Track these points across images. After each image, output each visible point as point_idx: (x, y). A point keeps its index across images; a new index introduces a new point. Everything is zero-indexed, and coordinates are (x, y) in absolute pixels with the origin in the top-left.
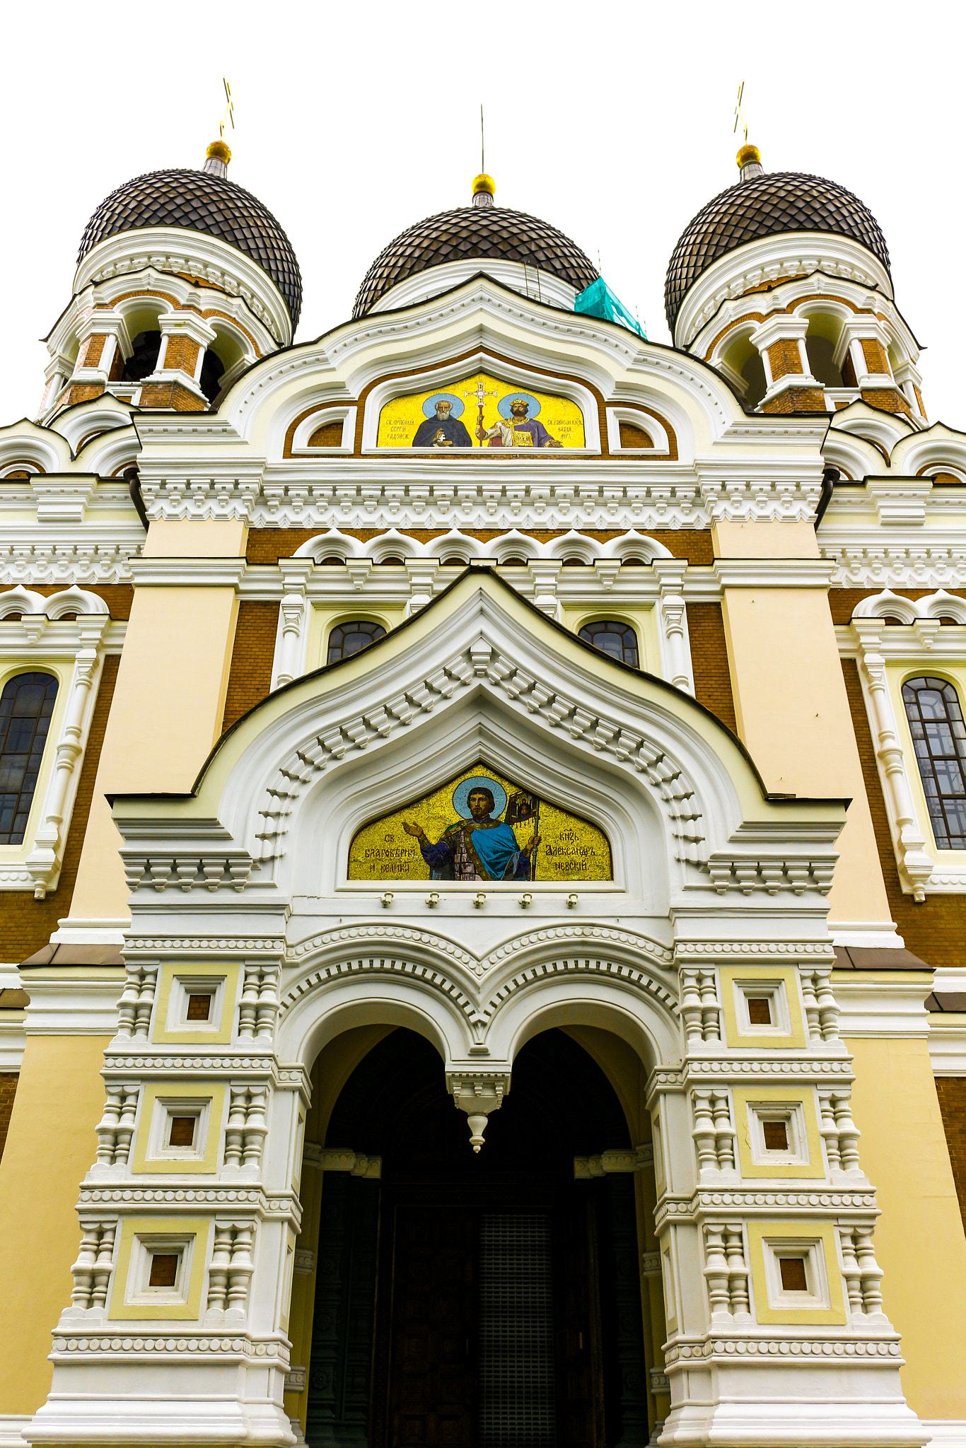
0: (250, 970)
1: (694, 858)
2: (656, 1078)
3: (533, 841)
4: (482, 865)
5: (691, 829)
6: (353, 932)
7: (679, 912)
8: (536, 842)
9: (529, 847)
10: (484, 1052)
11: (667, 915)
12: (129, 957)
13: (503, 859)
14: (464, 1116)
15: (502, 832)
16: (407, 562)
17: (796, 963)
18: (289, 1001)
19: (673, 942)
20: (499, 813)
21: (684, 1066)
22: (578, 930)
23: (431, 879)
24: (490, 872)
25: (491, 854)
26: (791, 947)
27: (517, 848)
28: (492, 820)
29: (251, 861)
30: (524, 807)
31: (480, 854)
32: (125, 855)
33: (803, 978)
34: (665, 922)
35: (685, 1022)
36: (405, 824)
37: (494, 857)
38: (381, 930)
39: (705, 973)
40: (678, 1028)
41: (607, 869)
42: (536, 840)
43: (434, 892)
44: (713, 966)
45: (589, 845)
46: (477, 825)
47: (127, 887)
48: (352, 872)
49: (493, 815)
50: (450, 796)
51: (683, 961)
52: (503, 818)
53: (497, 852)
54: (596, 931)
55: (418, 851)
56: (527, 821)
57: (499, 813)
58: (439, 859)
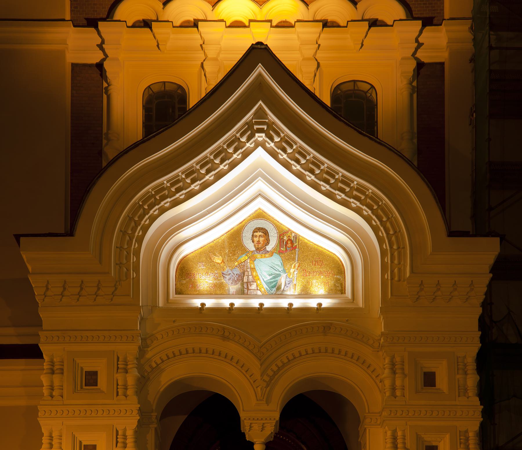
24: (267, 289)
28: (268, 252)
30: (289, 242)
46: (258, 256)
49: (269, 248)
53: (272, 275)
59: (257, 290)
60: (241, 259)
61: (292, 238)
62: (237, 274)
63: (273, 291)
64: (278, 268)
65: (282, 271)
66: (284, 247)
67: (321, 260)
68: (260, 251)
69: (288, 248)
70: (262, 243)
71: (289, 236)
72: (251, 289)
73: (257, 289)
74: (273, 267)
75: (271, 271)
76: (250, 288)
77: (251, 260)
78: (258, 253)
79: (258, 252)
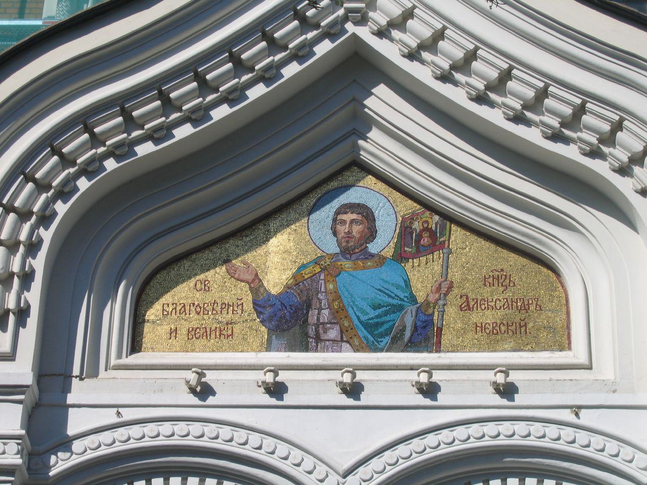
3: (439, 289)
9: (432, 298)
13: (388, 318)
15: (389, 274)
23: (268, 349)
25: (369, 310)
27: (413, 299)
28: (372, 255)
30: (426, 235)
31: (351, 311)
37: (373, 313)
42: (444, 288)
46: (347, 264)
49: (373, 248)
52: (389, 252)
53: (380, 306)
55: (249, 306)
56: (430, 257)
59: (342, 340)
60: (303, 272)
61: (434, 226)
65: (405, 299)
66: (414, 245)
67: (506, 276)
68: (351, 255)
69: (421, 249)
70: (357, 236)
72: (326, 338)
74: (383, 289)
75: (379, 297)
76: (324, 337)
77: (328, 275)
78: (347, 259)
79: (348, 256)
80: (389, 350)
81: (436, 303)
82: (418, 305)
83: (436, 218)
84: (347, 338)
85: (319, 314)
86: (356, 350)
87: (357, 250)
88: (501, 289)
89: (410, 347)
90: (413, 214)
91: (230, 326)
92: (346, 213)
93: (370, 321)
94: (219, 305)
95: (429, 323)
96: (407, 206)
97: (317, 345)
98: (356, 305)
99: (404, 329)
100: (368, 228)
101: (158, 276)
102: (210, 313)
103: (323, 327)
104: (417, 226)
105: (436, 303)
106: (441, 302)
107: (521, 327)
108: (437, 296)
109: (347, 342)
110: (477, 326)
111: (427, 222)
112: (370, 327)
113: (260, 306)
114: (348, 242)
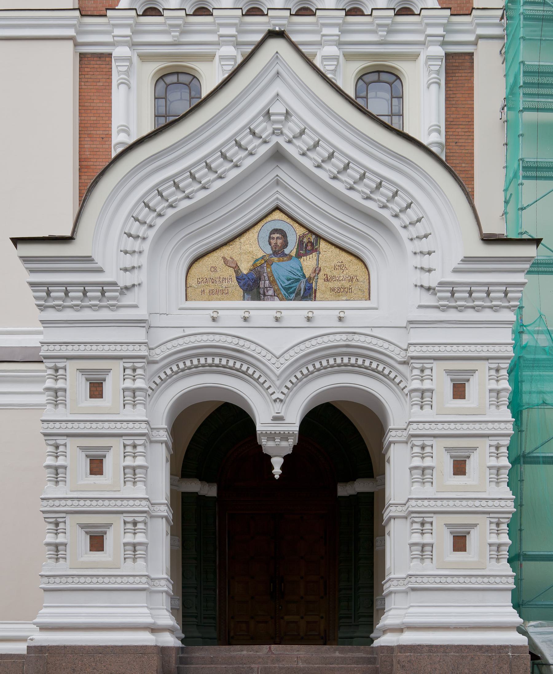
0: (127, 365)
1: (426, 285)
2: (390, 433)
3: (315, 271)
4: (279, 289)
5: (425, 261)
6: (193, 338)
7: (412, 323)
8: (317, 272)
9: (312, 276)
10: (281, 418)
11: (405, 325)
12: (46, 357)
13: (294, 285)
14: (269, 457)
15: (293, 263)
16: (215, 13)
17: (487, 359)
18: (154, 386)
19: (407, 344)
20: (291, 249)
21: (408, 426)
22: (344, 337)
24: (285, 295)
25: (286, 281)
26: (485, 348)
27: (304, 276)
28: (286, 255)
29: (119, 288)
30: (309, 244)
31: (277, 281)
32: (32, 284)
33: (490, 369)
34: (405, 329)
35: (411, 398)
36: (224, 258)
37: (287, 283)
38: (211, 337)
39: (426, 365)
40: (406, 402)
41: (367, 291)
42: (317, 271)
43: (247, 310)
44: (432, 361)
45: (355, 274)
46: (275, 259)
47: (36, 308)
48: (189, 295)
49: (287, 251)
50: (256, 236)
51: (412, 358)
52: (293, 254)
53: (290, 279)
54: (356, 337)
56: (311, 256)
57: (291, 249)
58: (249, 285)
61: (313, 240)
62: (252, 279)
63: (291, 297)
64: (298, 273)
65: (301, 276)
70: (280, 245)
71: (309, 238)
72: (268, 294)
73: (274, 294)
74: (291, 271)
76: (267, 294)
79: (276, 255)
80: (294, 300)
81: (315, 276)
82: (306, 279)
83: (314, 236)
84: (277, 295)
85: (264, 283)
86: (281, 300)
87: (280, 252)
88: (342, 271)
89: (303, 298)
90: (303, 234)
91: (227, 289)
92: (275, 234)
93: (286, 287)
94: (222, 279)
95: (310, 288)
96: (301, 231)
97: (264, 298)
98: (280, 279)
99: (300, 290)
100: (284, 241)
101: (194, 265)
102: (218, 282)
103: (267, 289)
104: (305, 240)
105: (314, 278)
106: (316, 278)
107: (349, 289)
108: (314, 274)
109: (277, 296)
110: (331, 289)
111: (309, 238)
112: (286, 289)
113: (238, 279)
114: (275, 248)
